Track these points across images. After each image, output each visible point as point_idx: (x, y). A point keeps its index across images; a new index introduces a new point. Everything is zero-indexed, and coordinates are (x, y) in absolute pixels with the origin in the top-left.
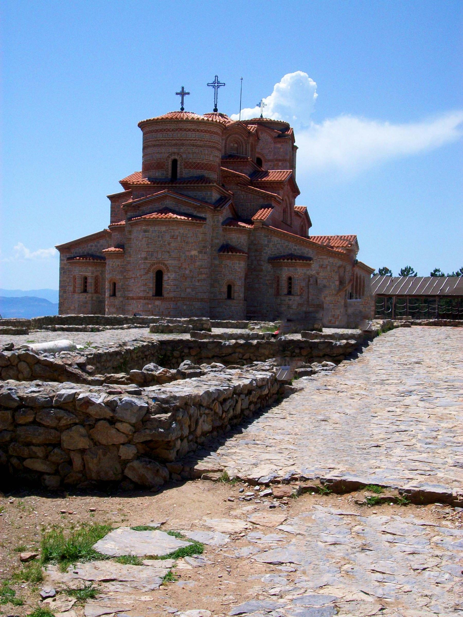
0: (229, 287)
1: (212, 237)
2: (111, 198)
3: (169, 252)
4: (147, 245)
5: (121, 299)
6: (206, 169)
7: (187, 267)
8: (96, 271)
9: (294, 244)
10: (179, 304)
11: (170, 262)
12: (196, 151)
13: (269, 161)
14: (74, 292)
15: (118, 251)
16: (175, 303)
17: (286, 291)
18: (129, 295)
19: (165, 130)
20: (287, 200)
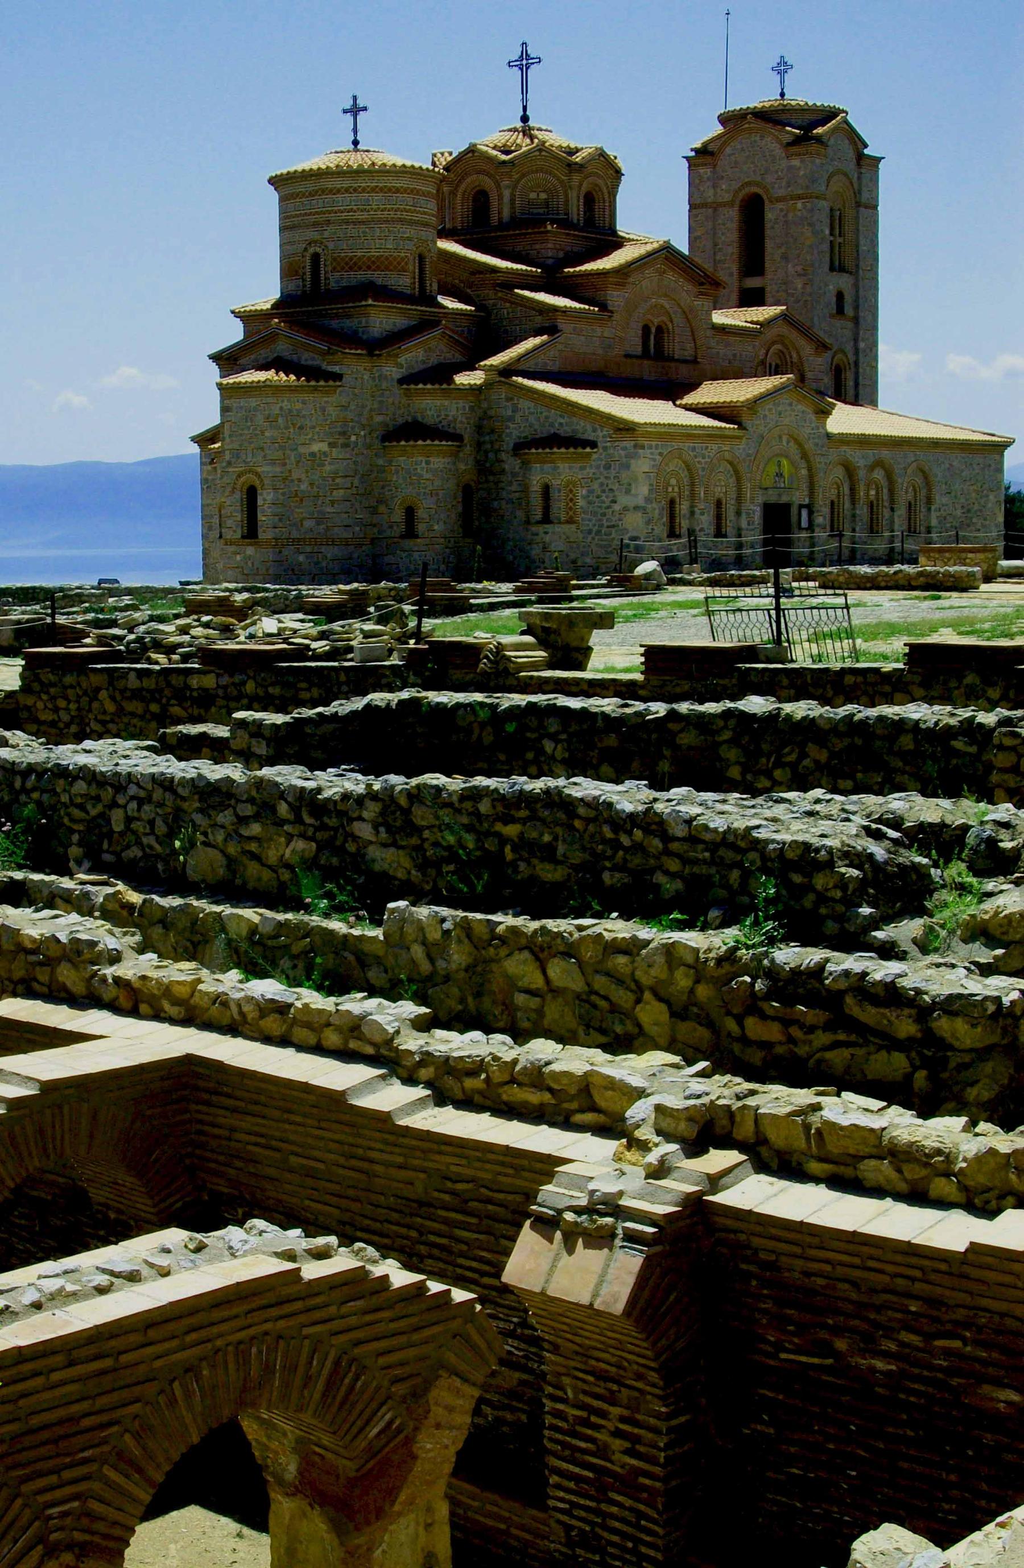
0: (410, 512)
1: (371, 410)
3: (262, 449)
6: (378, 268)
7: (303, 477)
10: (285, 552)
11: (264, 469)
13: (779, 200)
17: (538, 515)
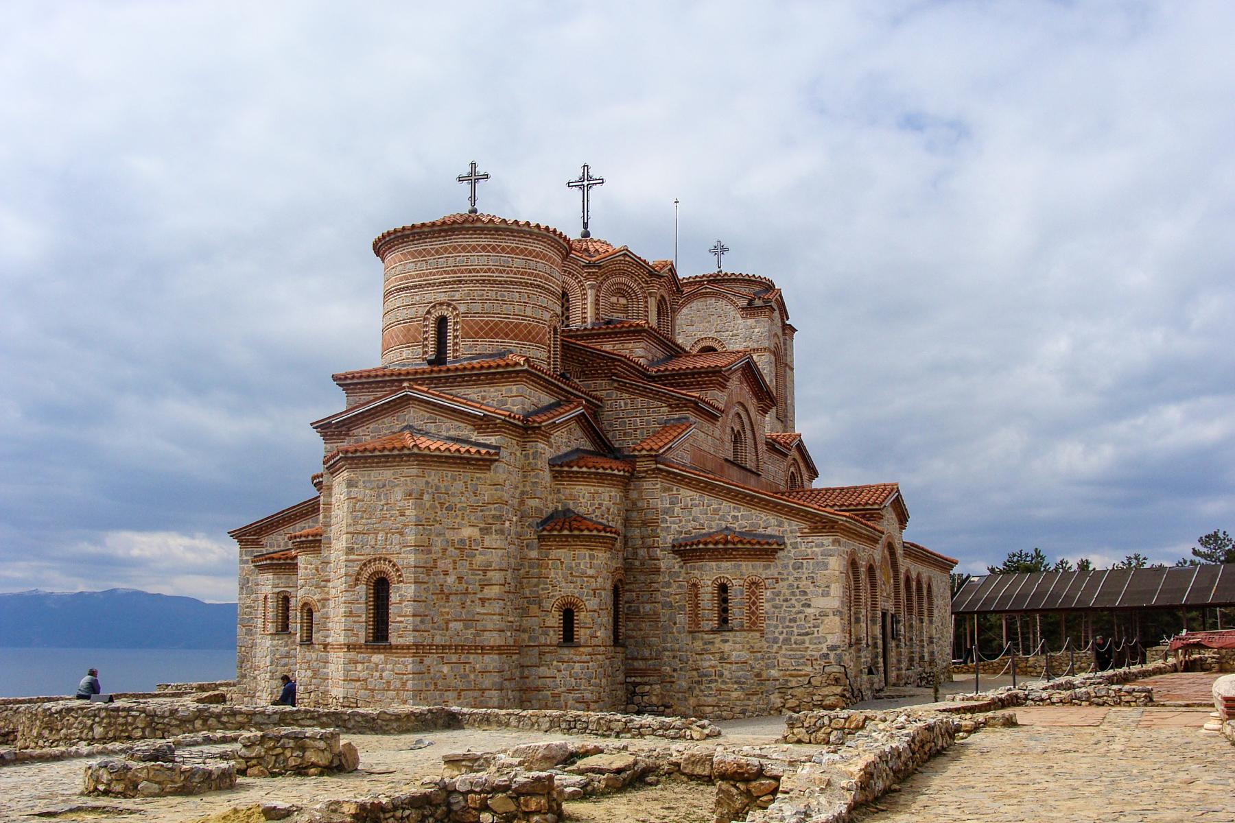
0: (568, 615)
1: (523, 493)
3: (401, 534)
6: (516, 337)
7: (451, 566)
9: (732, 505)
12: (492, 295)
16: (418, 659)
20: (743, 415)
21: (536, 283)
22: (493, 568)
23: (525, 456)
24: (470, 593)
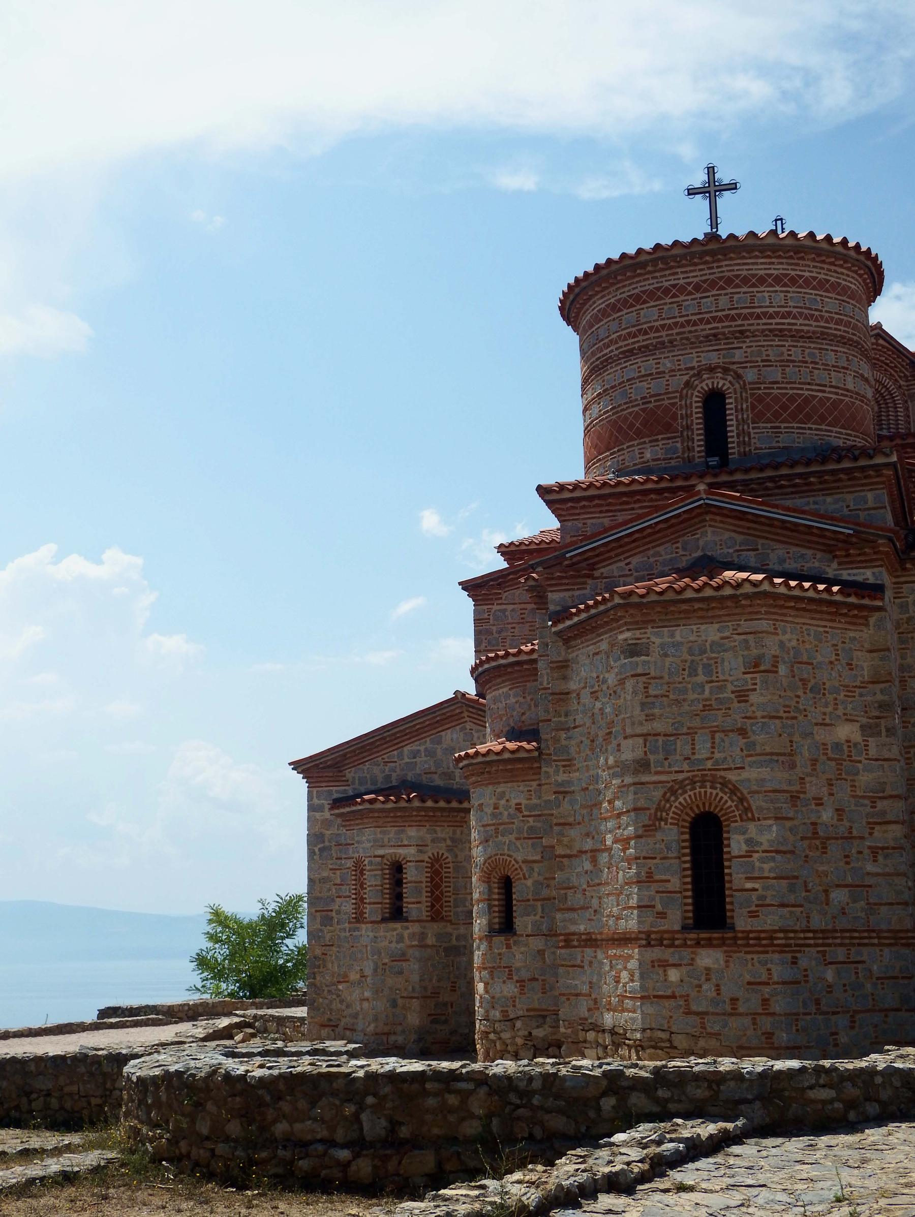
2: (473, 587)
3: (742, 732)
4: (643, 704)
5: (537, 943)
7: (825, 790)
8: (433, 841)
10: (803, 962)
12: (796, 354)
14: (359, 918)
15: (513, 752)
16: (789, 956)
18: (573, 928)
19: (667, 291)
21: (855, 338)
22: (886, 794)
23: (901, 606)
24: (855, 838)
